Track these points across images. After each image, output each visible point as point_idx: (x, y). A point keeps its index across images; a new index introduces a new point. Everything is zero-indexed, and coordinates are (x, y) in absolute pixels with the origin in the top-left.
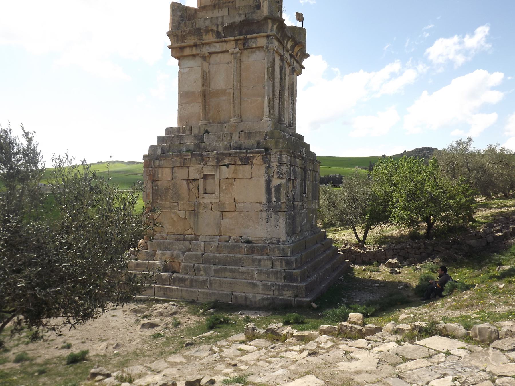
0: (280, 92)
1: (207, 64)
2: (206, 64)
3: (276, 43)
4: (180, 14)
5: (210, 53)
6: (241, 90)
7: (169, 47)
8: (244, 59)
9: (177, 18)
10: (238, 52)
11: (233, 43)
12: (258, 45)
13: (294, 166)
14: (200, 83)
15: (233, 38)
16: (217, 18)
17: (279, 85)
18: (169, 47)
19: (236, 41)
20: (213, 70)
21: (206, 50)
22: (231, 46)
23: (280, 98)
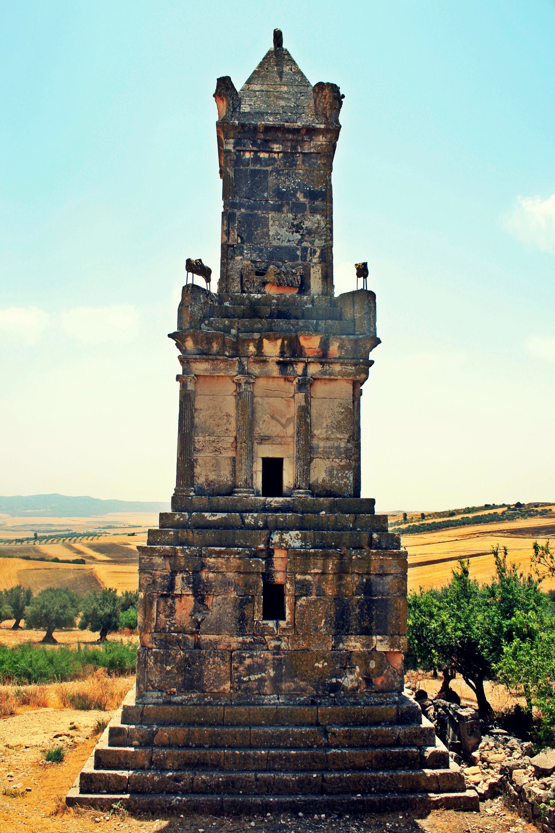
13: (196, 572)
17: (233, 426)
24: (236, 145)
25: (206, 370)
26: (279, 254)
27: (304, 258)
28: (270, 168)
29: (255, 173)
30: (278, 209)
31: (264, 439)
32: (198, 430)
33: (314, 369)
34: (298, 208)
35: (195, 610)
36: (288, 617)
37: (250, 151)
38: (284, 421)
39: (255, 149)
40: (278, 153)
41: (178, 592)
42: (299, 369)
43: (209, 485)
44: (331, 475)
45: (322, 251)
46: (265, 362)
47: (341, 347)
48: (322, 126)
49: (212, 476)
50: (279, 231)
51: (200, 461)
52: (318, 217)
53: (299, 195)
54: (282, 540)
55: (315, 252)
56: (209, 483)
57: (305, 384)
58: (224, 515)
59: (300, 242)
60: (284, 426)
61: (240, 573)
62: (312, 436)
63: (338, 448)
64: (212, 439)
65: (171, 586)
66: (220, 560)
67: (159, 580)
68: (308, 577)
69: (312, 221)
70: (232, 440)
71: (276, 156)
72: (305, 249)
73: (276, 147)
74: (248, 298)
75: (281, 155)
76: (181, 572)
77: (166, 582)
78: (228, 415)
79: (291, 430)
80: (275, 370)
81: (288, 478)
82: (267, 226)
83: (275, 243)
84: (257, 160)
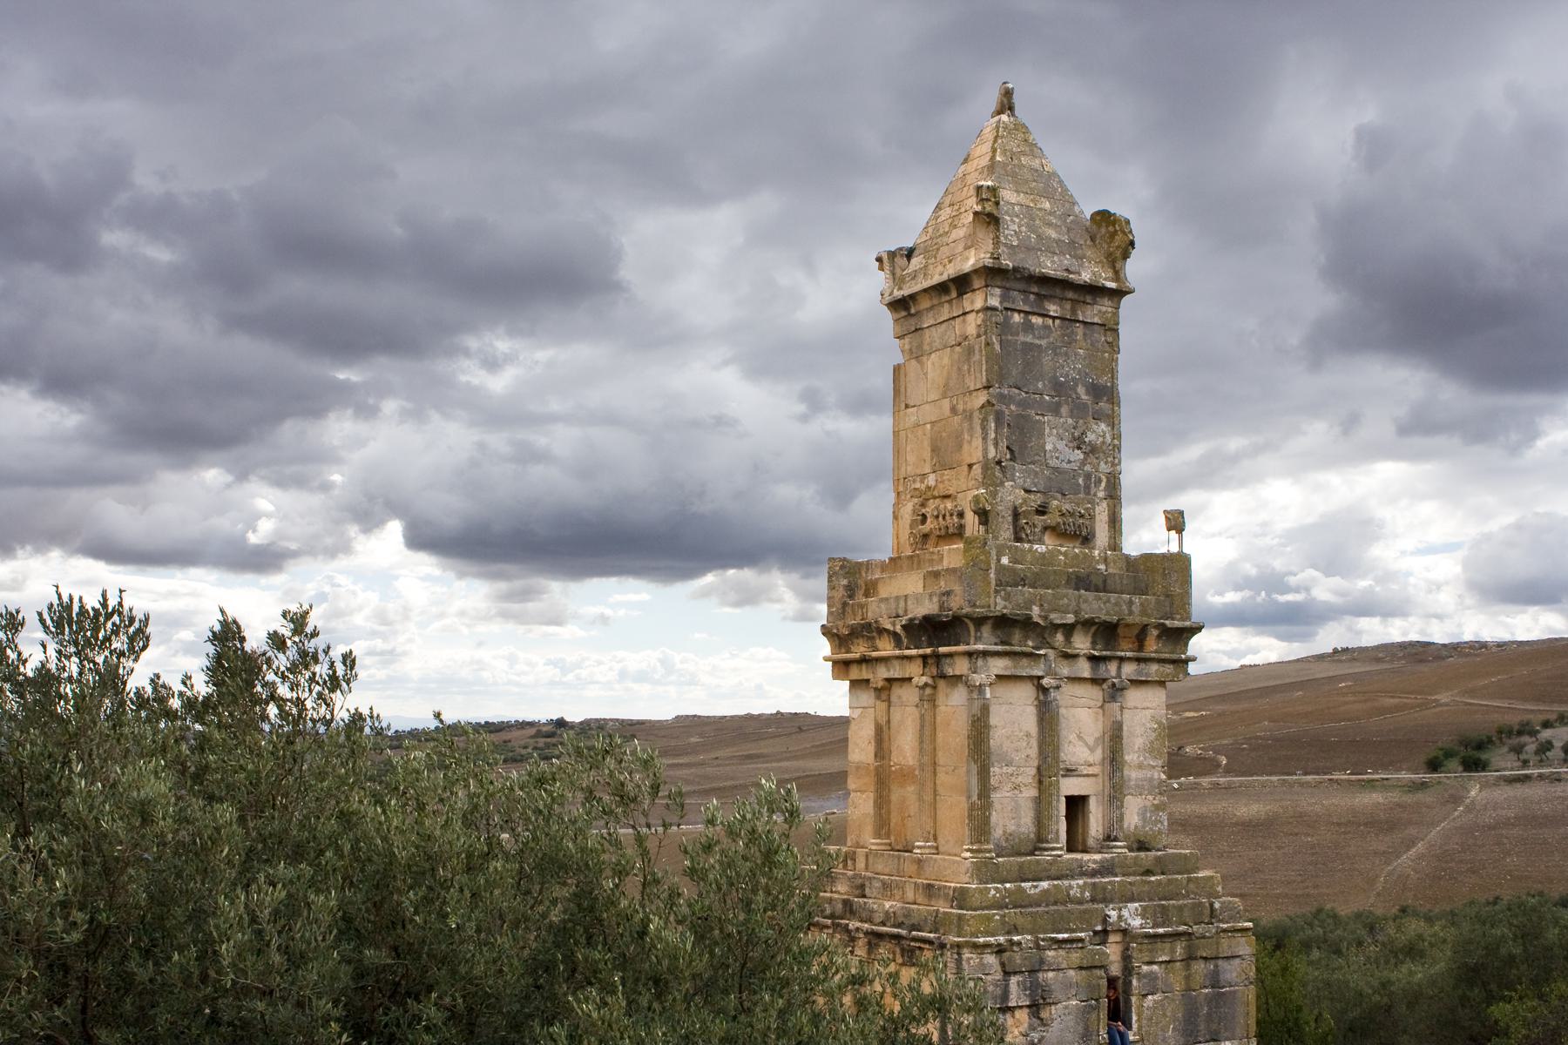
0: (1039, 769)
1: (884, 705)
2: (882, 706)
3: (999, 666)
4: (845, 582)
5: (889, 680)
6: (935, 773)
7: (826, 659)
8: (941, 699)
9: (840, 593)
10: (926, 685)
11: (919, 662)
12: (958, 673)
14: (871, 749)
15: (914, 652)
16: (897, 598)
18: (826, 659)
19: (924, 657)
20: (896, 715)
21: (883, 673)
22: (914, 670)
23: (1040, 782)
24: (1003, 298)
25: (1006, 668)
26: (1061, 483)
27: (1087, 487)
28: (1043, 342)
29: (1028, 347)
30: (1056, 410)
31: (1070, 772)
32: (993, 758)
33: (1129, 670)
34: (1079, 411)
35: (1032, 1028)
36: (1135, 1026)
37: (1020, 312)
38: (1091, 741)
39: (1027, 309)
40: (1054, 318)
41: (1012, 1004)
42: (1112, 668)
43: (1007, 840)
44: (1144, 819)
45: (1108, 481)
46: (1075, 656)
47: (1159, 637)
48: (1112, 285)
49: (1011, 828)
50: (1056, 445)
51: (997, 805)
52: (1103, 426)
53: (1081, 390)
54: (1120, 917)
55: (1100, 481)
56: (1008, 836)
57: (1115, 692)
58: (1045, 885)
59: (1083, 463)
60: (1092, 750)
61: (1081, 968)
62: (1123, 763)
63: (1151, 779)
64: (1010, 770)
65: (1005, 995)
66: (1062, 952)
67: (991, 989)
68: (1155, 967)
69: (1098, 432)
70: (1033, 771)
71: (1050, 322)
72: (1088, 476)
73: (1053, 309)
74: (1030, 550)
75: (1057, 322)
76: (1015, 973)
77: (999, 991)
78: (1028, 735)
79: (1098, 755)
80: (1084, 669)
81: (1095, 824)
82: (1041, 435)
83: (1053, 463)
84: (1028, 327)
